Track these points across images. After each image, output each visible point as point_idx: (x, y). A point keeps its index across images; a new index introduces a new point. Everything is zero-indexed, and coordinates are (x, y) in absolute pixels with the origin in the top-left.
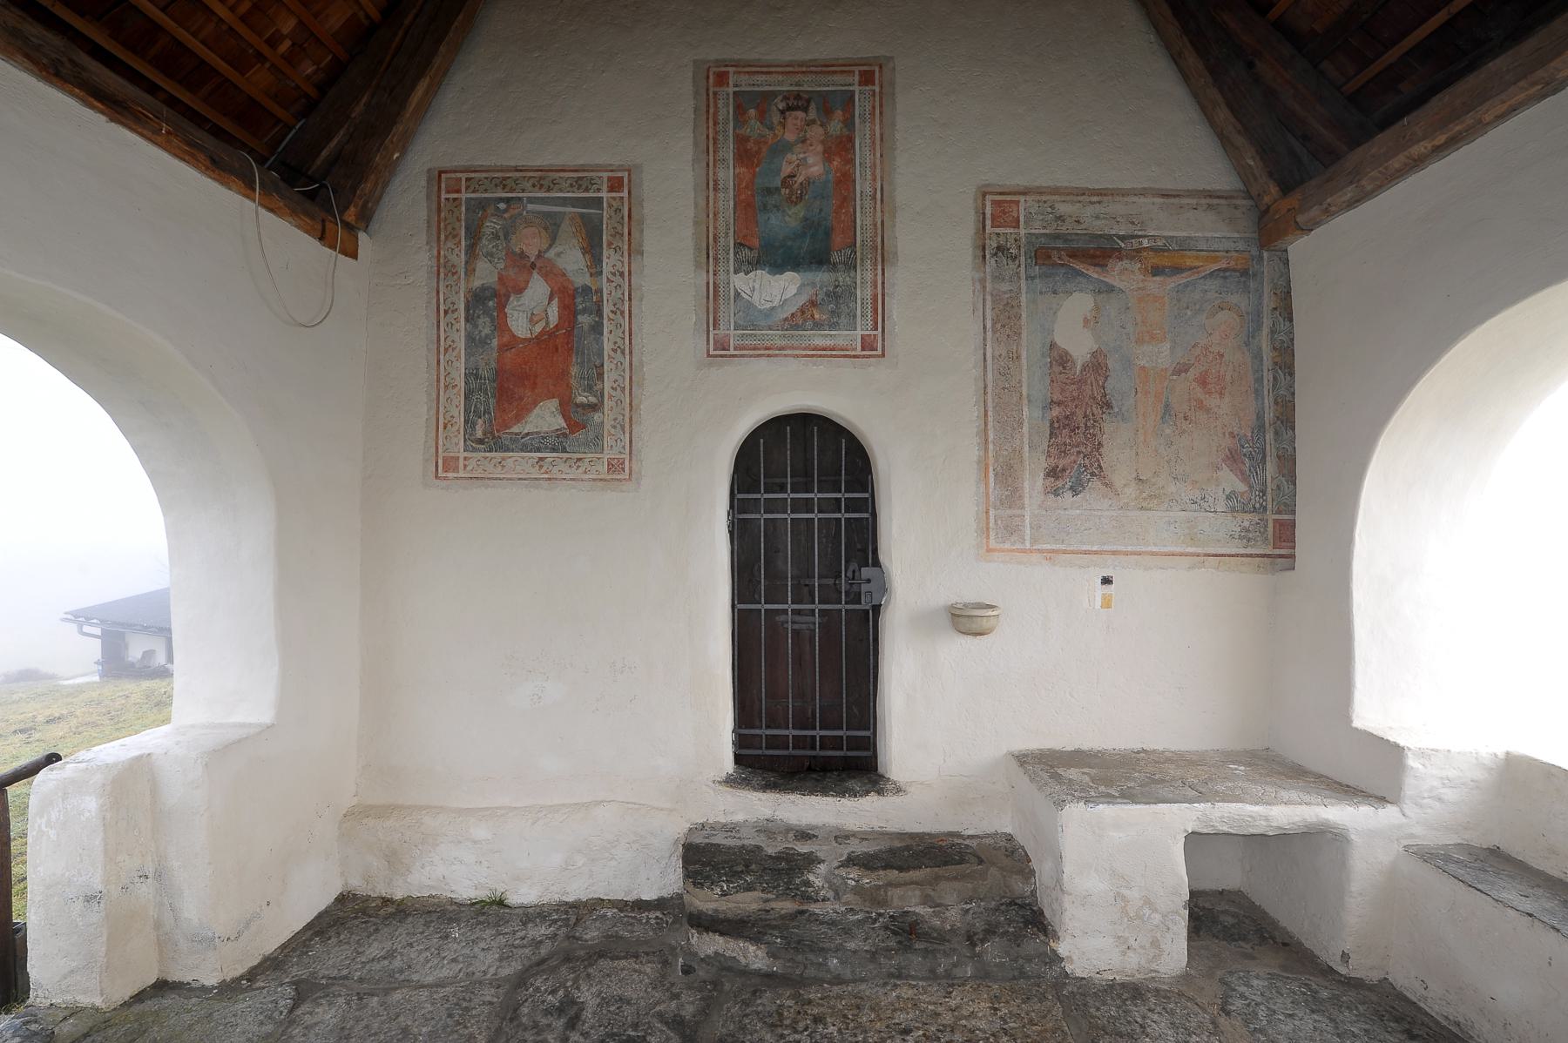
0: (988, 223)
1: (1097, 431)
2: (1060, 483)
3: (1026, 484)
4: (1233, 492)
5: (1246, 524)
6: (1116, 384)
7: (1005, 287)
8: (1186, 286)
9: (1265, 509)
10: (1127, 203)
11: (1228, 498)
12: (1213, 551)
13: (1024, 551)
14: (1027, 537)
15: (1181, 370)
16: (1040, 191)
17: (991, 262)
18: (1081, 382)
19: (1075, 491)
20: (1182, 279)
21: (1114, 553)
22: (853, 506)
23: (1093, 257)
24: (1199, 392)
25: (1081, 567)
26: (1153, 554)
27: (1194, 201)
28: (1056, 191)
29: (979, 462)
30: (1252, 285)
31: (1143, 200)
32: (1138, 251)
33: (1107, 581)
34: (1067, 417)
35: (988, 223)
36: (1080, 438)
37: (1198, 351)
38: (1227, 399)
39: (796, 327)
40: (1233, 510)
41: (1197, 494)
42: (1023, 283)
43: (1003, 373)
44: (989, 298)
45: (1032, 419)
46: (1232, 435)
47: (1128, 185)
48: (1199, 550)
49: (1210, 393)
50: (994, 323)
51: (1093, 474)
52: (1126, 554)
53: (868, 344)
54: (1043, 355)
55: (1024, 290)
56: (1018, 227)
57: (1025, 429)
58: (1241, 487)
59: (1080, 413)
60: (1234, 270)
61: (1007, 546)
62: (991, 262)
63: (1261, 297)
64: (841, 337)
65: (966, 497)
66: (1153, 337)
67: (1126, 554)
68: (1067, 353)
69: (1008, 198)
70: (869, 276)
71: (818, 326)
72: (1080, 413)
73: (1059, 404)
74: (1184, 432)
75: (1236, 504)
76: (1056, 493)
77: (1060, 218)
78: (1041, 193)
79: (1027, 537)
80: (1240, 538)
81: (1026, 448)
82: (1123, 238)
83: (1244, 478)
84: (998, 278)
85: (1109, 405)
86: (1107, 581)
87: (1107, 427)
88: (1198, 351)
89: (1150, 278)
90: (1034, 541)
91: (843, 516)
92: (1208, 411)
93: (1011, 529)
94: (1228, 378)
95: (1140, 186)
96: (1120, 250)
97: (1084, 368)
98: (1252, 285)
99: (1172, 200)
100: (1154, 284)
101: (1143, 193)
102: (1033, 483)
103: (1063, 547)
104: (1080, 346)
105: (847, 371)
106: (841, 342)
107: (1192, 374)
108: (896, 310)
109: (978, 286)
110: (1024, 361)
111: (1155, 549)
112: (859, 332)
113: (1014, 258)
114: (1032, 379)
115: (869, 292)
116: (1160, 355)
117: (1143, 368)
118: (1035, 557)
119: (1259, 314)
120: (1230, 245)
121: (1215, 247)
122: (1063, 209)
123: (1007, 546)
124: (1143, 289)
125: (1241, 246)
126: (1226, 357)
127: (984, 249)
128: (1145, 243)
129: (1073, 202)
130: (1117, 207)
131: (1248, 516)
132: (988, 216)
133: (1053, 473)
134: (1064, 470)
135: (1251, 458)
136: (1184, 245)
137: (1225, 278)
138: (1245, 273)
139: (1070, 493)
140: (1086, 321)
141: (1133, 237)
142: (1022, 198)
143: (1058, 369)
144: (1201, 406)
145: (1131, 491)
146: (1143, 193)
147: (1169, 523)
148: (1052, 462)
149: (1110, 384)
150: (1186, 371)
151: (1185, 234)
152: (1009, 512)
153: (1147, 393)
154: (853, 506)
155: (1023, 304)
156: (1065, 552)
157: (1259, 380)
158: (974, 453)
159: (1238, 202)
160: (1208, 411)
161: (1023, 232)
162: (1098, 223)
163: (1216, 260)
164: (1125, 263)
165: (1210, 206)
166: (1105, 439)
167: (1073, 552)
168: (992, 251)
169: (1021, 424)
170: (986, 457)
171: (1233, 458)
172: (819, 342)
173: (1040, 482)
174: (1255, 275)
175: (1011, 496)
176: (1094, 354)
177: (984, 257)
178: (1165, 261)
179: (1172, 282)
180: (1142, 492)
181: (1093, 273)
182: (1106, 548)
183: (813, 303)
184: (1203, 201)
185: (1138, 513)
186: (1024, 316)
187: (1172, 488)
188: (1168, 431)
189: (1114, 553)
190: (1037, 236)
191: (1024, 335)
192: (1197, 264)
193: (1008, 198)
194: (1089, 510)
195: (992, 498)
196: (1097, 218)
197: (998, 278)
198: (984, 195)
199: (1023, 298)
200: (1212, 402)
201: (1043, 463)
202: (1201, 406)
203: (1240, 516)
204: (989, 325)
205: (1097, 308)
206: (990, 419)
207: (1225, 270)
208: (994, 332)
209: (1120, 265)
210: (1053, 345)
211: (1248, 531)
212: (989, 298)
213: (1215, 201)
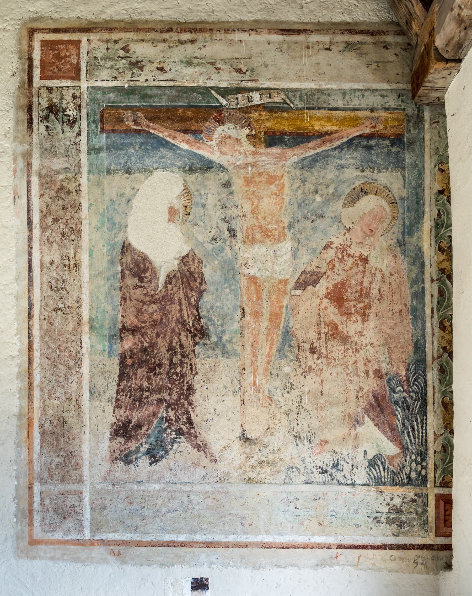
0: (37, 72)
1: (186, 370)
2: (132, 445)
3: (86, 449)
4: (378, 456)
5: (397, 501)
7: (58, 163)
8: (315, 159)
9: (424, 480)
10: (231, 43)
11: (372, 464)
12: (349, 541)
13: (80, 543)
14: (87, 524)
15: (308, 280)
16: (109, 27)
17: (40, 128)
18: (165, 300)
19: (154, 456)
20: (309, 151)
21: (209, 545)
23: (182, 119)
24: (332, 313)
25: (162, 565)
26: (265, 546)
27: (326, 39)
28: (133, 26)
29: (20, 416)
30: (408, 158)
31: (254, 37)
32: (246, 110)
34: (144, 350)
35: (37, 72)
36: (161, 380)
37: (331, 254)
38: (372, 323)
40: (378, 482)
42: (84, 158)
43: (57, 288)
44: (35, 180)
46: (378, 374)
47: (235, 17)
48: (330, 540)
49: (348, 314)
50: (44, 217)
51: (180, 432)
52: (226, 546)
54: (112, 262)
55: (85, 170)
56: (77, 77)
57: (85, 368)
58: (390, 449)
59: (162, 345)
60: (382, 137)
61: (58, 535)
62: (40, 128)
63: (420, 174)
66: (267, 234)
67: (226, 546)
68: (145, 259)
69: (65, 37)
72: (162, 345)
73: (134, 331)
74: (310, 369)
75: (382, 473)
76: (127, 459)
77: (137, 65)
78: (110, 30)
79: (87, 524)
80: (390, 522)
81: (86, 395)
82: (224, 92)
83: (395, 436)
84: (49, 151)
85: (203, 333)
86: (200, 584)
88: (331, 254)
89: (262, 150)
90: (96, 527)
92: (345, 339)
93: (64, 512)
94: (374, 292)
95: (249, 17)
96: (219, 109)
97: (169, 280)
98: (408, 158)
99: (295, 38)
100: (269, 157)
101: (254, 27)
103: (135, 537)
104: (164, 248)
107: (323, 286)
109: (21, 163)
110: (85, 270)
111: (268, 539)
113: (72, 123)
116: (274, 261)
117: (253, 280)
118: (98, 551)
119: (418, 200)
120: (373, 100)
121: (356, 103)
122: (141, 50)
123: (58, 535)
124: (253, 165)
125: (392, 102)
126: (372, 262)
127: (30, 109)
128: (257, 98)
129: (153, 41)
130: (217, 48)
131: (400, 491)
132: (37, 62)
133: (123, 430)
134: (139, 426)
135: (406, 406)
136: (313, 101)
137: (369, 148)
138: (397, 140)
139: (144, 462)
140: (172, 212)
141: (239, 90)
142: (84, 38)
143: (131, 281)
144: (335, 333)
146: (254, 27)
147: (288, 502)
148: (122, 414)
150: (315, 283)
151: (312, 85)
152: (61, 487)
153: (257, 314)
155: (84, 189)
156: (139, 544)
157: (419, 296)
159: (390, 39)
160: (345, 339)
161: (84, 85)
162: (189, 70)
163: (355, 122)
164: (228, 129)
165: (349, 46)
166: (197, 382)
167: (151, 544)
168: (41, 114)
169: (79, 361)
170: (30, 409)
171: (378, 406)
173: (105, 445)
174: (411, 143)
176: (184, 260)
177: (30, 122)
178: (282, 127)
179: (295, 155)
180: (248, 458)
181: (183, 143)
182: (198, 537)
184: (340, 38)
185: (245, 487)
186: (85, 205)
188: (287, 369)
189: (209, 545)
190: (104, 91)
191: (85, 235)
192: (329, 127)
193: (65, 37)
195: (37, 468)
196: (189, 63)
197: (49, 151)
198: (31, 32)
199: (84, 180)
200: (352, 327)
202: (335, 333)
203: (388, 490)
204: (36, 219)
206: (36, 354)
207: (370, 137)
208: (44, 228)
209: (220, 131)
210: (126, 248)
211: (399, 511)
212: (35, 180)
213: (357, 38)
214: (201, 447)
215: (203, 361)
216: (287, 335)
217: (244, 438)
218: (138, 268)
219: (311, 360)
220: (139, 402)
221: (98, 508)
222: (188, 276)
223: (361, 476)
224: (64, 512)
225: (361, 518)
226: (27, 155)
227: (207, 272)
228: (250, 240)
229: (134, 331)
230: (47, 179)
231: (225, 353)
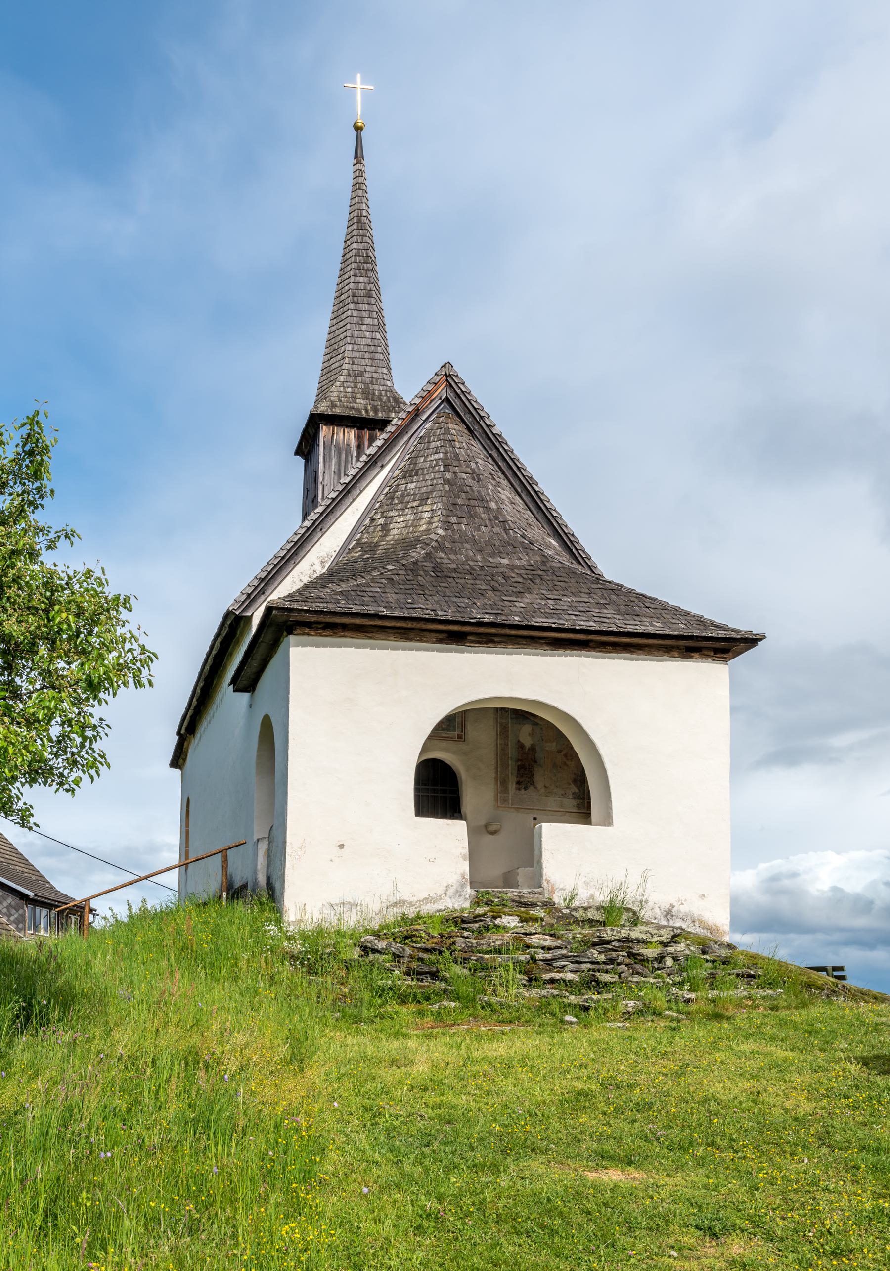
7: (504, 721)
15: (559, 752)
19: (525, 789)
33: (535, 819)
40: (574, 798)
43: (503, 749)
53: (460, 737)
58: (577, 791)
64: (451, 734)
76: (519, 789)
83: (578, 788)
85: (535, 762)
86: (535, 819)
93: (505, 800)
102: (512, 786)
104: (527, 742)
107: (562, 754)
108: (469, 728)
112: (457, 733)
133: (518, 783)
145: (543, 790)
158: (494, 775)
173: (514, 786)
175: (505, 790)
194: (529, 794)
200: (569, 763)
201: (515, 779)
210: (519, 741)
214: (536, 788)
215: (536, 769)
218: (521, 746)
220: (522, 776)
222: (533, 749)
223: (571, 796)
227: (537, 748)
230: (501, 724)
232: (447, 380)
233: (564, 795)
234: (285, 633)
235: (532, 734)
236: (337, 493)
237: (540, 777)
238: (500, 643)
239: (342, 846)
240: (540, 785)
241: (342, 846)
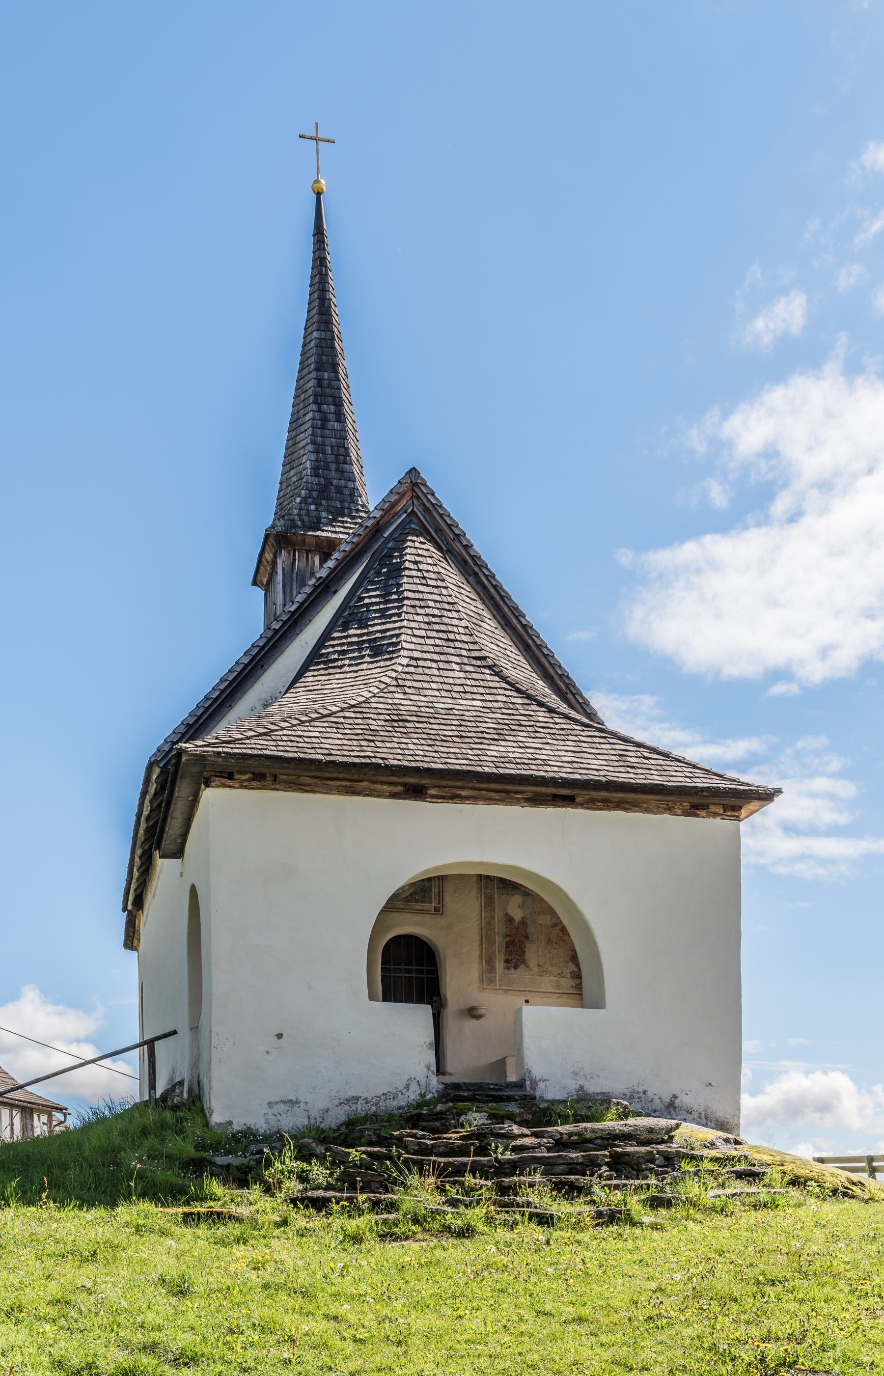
6: (531, 929)
7: (489, 891)
18: (517, 928)
19: (516, 967)
22: (429, 972)
39: (409, 901)
40: (573, 977)
41: (560, 971)
43: (489, 923)
45: (499, 941)
53: (437, 909)
62: (484, 881)
64: (426, 906)
65: (474, 970)
70: (437, 884)
71: (417, 901)
73: (509, 936)
76: (508, 968)
84: (486, 888)
85: (527, 937)
87: (527, 945)
90: (500, 985)
91: (425, 976)
93: (491, 981)
102: (499, 965)
104: (517, 915)
105: (428, 919)
106: (426, 908)
107: (558, 927)
108: (448, 898)
114: (499, 926)
115: (437, 890)
118: (500, 992)
133: (507, 961)
140: (519, 906)
144: (562, 939)
145: (536, 969)
149: (528, 929)
154: (429, 972)
158: (478, 953)
169: (495, 943)
172: (417, 907)
173: (502, 964)
183: (415, 893)
187: (551, 969)
194: (520, 975)
197: (486, 888)
201: (503, 957)
202: (562, 939)
205: (523, 901)
210: (507, 914)
216: (549, 939)
217: (539, 965)
218: (510, 920)
219: (555, 946)
220: (511, 954)
221: (500, 981)
222: (523, 922)
224: (491, 981)
225: (569, 986)
226: (480, 888)
228: (539, 914)
229: (509, 936)
230: (486, 895)
231: (534, 943)
232: (413, 490)
233: (561, 975)
234: (203, 786)
235: (522, 906)
236: (280, 624)
237: (532, 954)
238: (468, 798)
239: (280, 1036)
240: (532, 963)
241: (280, 1036)
